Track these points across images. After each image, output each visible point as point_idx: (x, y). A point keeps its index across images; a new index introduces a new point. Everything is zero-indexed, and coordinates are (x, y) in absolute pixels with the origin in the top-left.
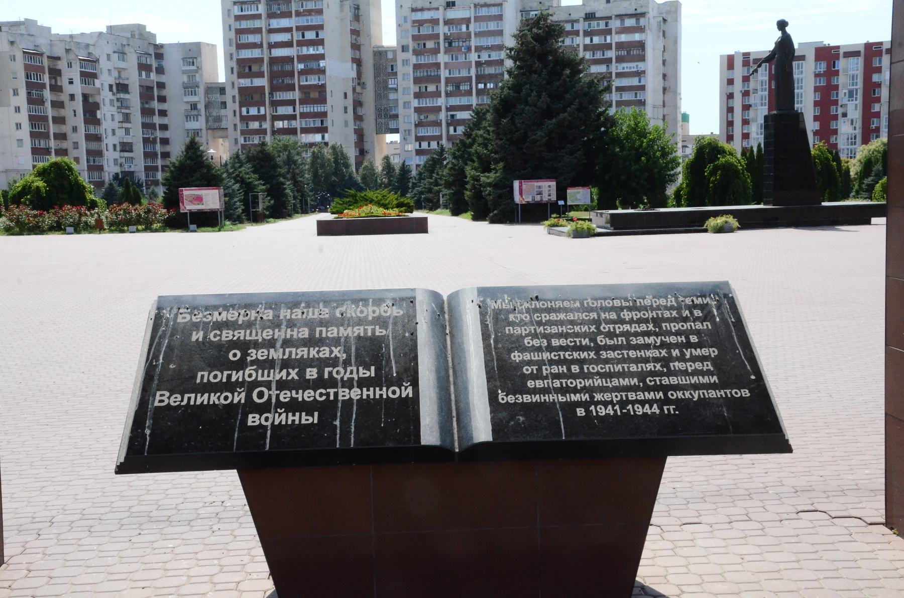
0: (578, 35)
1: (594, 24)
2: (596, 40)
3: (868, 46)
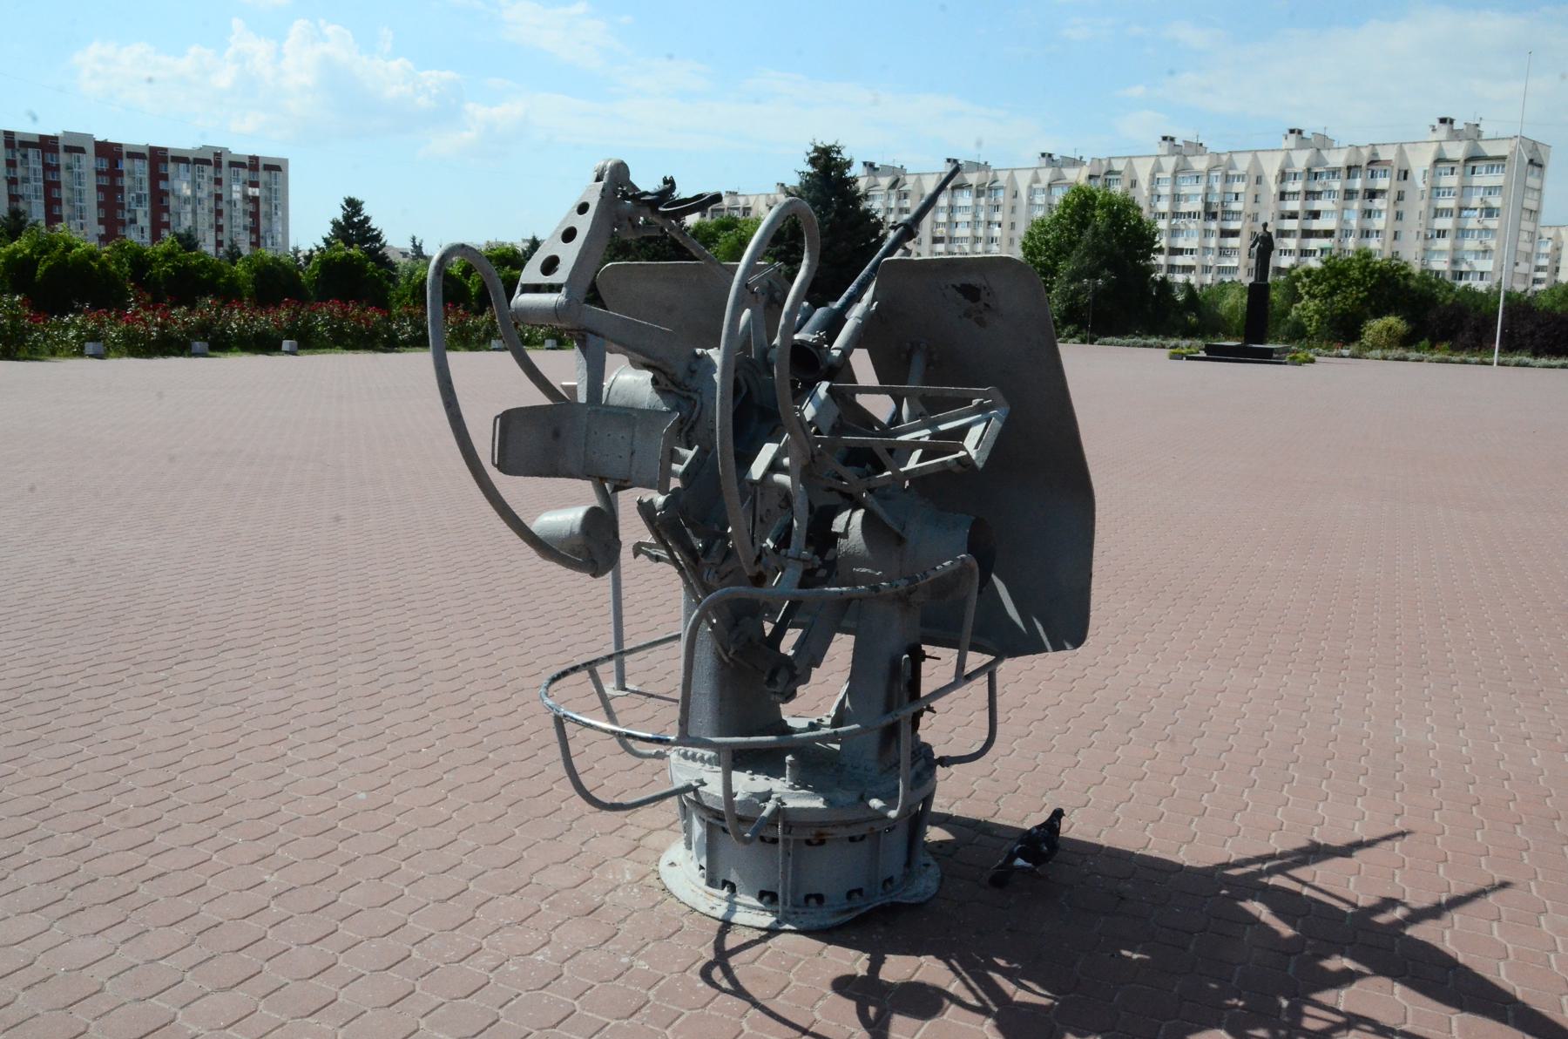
3: (153, 150)
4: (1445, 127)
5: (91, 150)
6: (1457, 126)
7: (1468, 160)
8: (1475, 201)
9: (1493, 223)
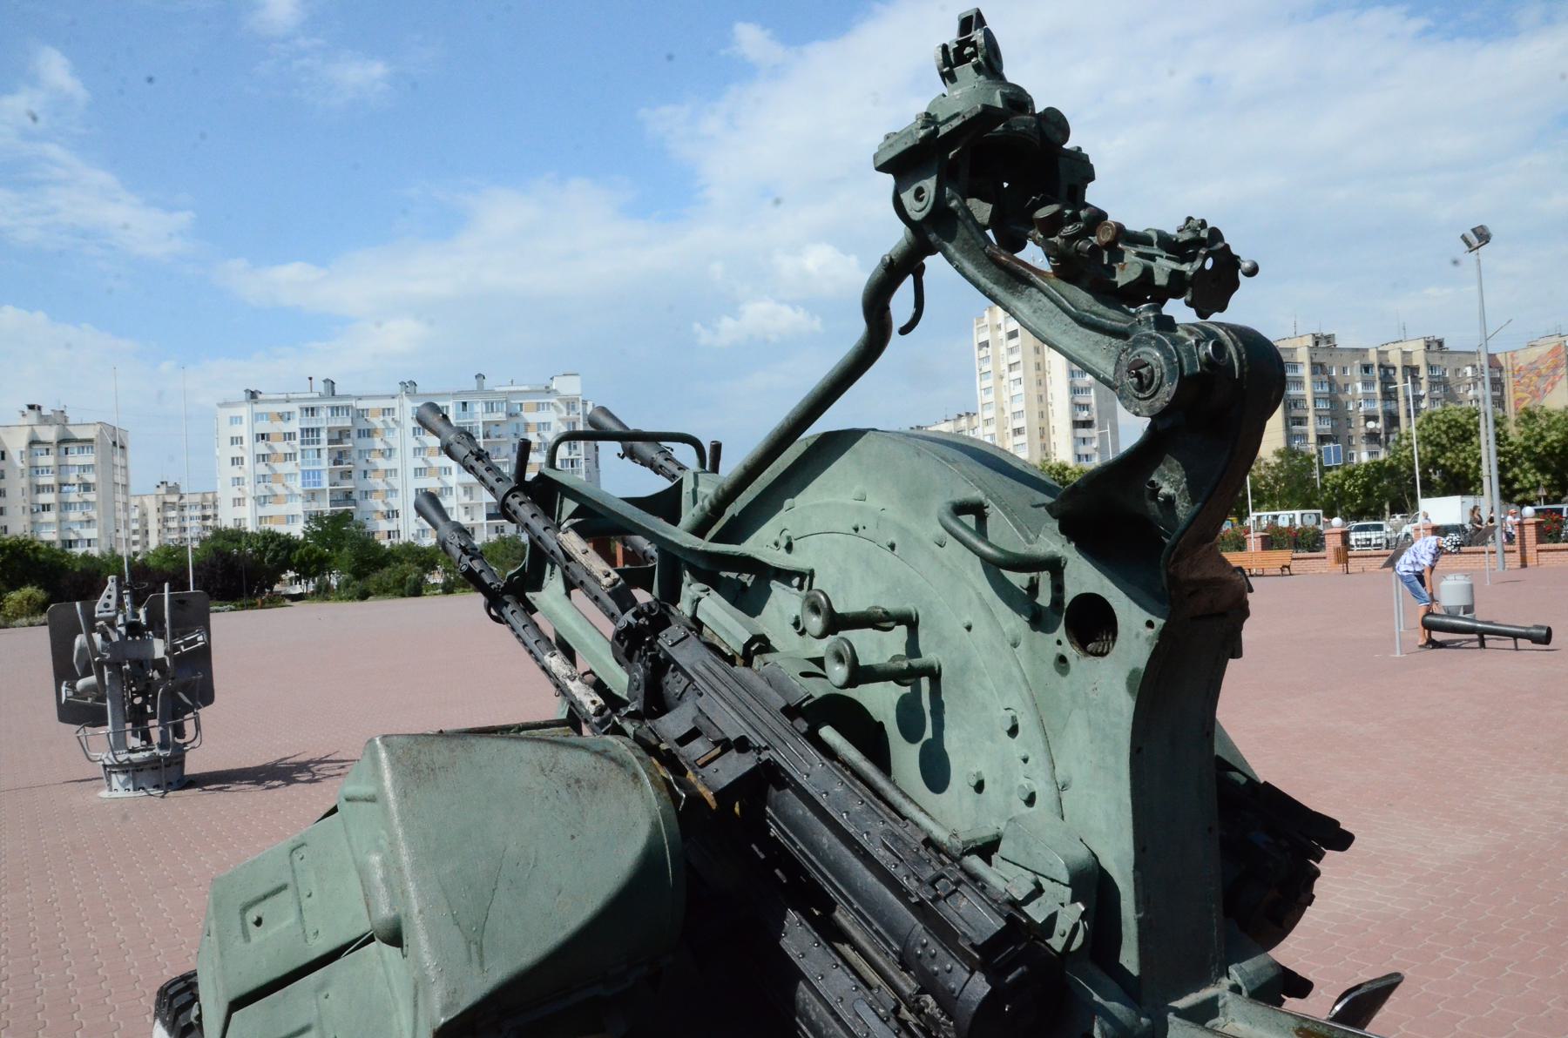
4: (34, 414)
6: (45, 412)
7: (61, 442)
8: (73, 478)
9: (91, 497)
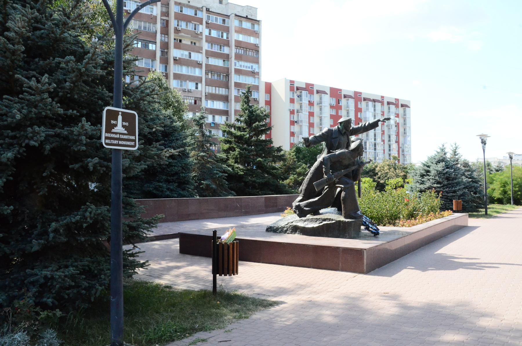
0: (201, 23)
1: (213, 17)
2: (214, 34)
3: (356, 93)
5: (328, 92)
